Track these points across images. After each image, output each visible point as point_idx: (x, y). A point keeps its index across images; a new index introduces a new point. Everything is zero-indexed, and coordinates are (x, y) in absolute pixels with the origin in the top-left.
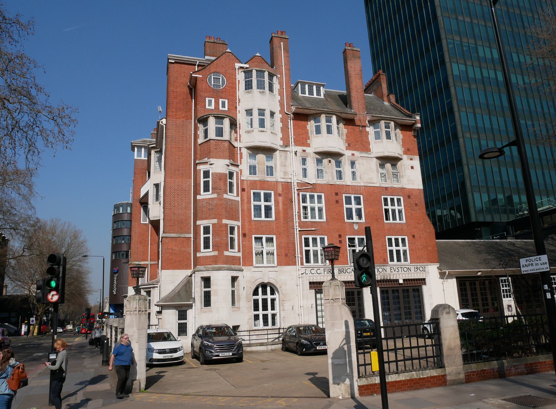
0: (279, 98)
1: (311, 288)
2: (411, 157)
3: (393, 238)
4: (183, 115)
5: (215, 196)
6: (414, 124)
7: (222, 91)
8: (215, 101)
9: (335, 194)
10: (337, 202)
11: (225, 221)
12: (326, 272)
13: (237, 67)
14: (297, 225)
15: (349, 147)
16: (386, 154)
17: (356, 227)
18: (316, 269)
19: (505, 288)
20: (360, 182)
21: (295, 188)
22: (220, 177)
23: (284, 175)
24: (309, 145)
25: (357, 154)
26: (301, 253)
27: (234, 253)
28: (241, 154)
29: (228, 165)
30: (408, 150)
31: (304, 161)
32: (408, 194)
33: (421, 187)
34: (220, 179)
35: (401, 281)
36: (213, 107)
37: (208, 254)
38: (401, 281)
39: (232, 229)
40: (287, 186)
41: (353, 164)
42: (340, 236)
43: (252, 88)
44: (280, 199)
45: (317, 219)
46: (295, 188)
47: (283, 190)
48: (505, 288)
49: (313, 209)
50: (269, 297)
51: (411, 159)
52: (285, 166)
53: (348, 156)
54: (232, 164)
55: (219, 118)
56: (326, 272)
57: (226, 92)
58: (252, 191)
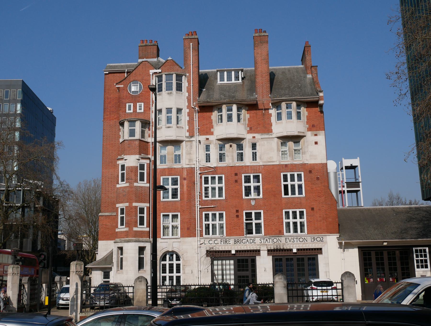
0: (187, 94)
2: (315, 132)
4: (116, 117)
7: (139, 96)
9: (234, 173)
11: (134, 204)
12: (222, 243)
13: (151, 74)
14: (198, 203)
15: (251, 130)
16: (285, 134)
17: (253, 203)
18: (214, 240)
19: (420, 258)
20: (259, 162)
21: (198, 172)
22: (133, 169)
23: (189, 162)
24: (212, 134)
25: (258, 136)
26: (201, 227)
29: (139, 160)
31: (208, 148)
34: (132, 171)
35: (295, 251)
37: (122, 230)
38: (295, 251)
39: (142, 211)
40: (191, 171)
41: (254, 146)
42: (237, 211)
43: (162, 91)
44: (185, 182)
45: (217, 198)
46: (198, 172)
47: (187, 175)
48: (420, 258)
49: (213, 189)
50: (175, 262)
51: (316, 135)
52: (190, 154)
53: (249, 139)
54: (142, 158)
56: (222, 243)
57: (142, 96)
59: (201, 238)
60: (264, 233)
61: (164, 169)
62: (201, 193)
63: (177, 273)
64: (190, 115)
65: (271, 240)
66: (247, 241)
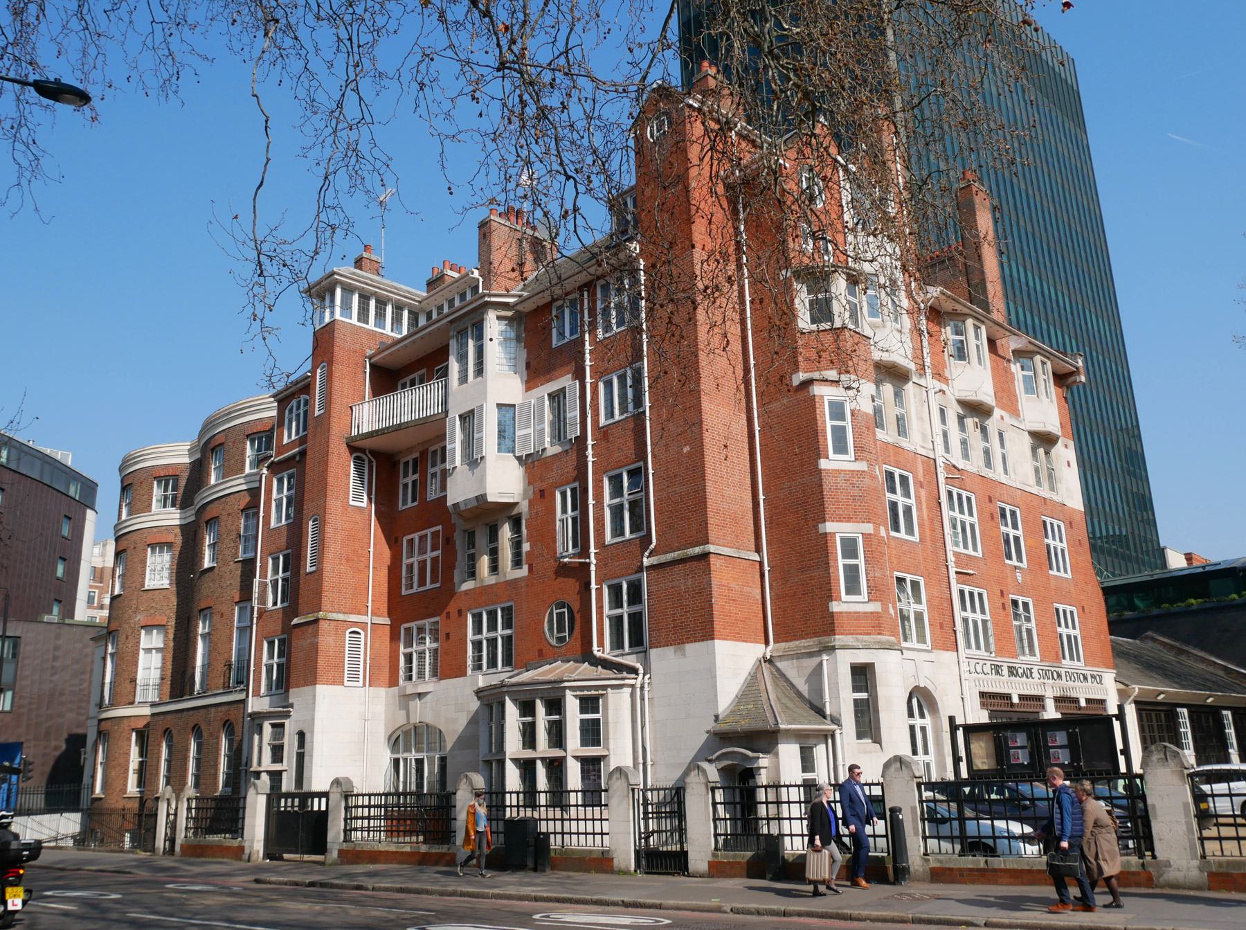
6: (1072, 374)
33: (1082, 509)
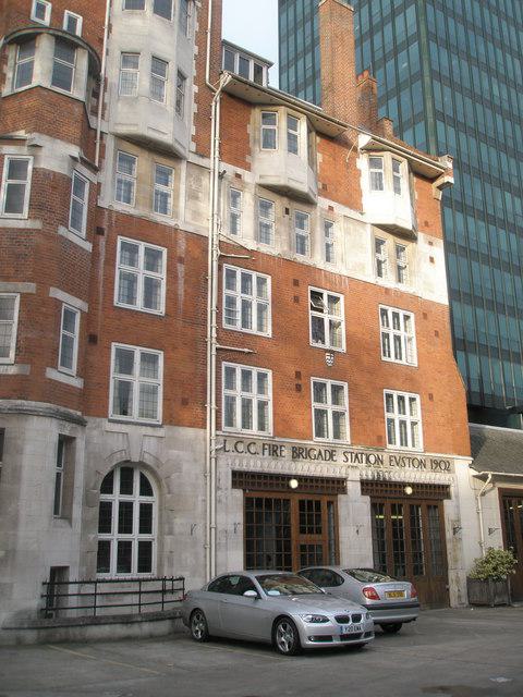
1: (235, 485)
3: (395, 394)
5: (37, 225)
8: (53, 10)
10: (296, 299)
11: (56, 293)
12: (266, 452)
14: (214, 335)
17: (328, 358)
21: (213, 254)
24: (248, 167)
25: (340, 210)
27: (66, 375)
28: (103, 147)
30: (426, 224)
32: (424, 311)
36: (47, 21)
40: (199, 241)
42: (298, 375)
46: (213, 254)
50: (137, 499)
51: (431, 243)
53: (322, 209)
55: (65, 44)
56: (266, 452)
58: (120, 239)
59: (218, 433)
60: (352, 439)
61: (131, 216)
62: (219, 307)
63: (141, 532)
64: (203, 100)
65: (364, 457)
66: (320, 453)
